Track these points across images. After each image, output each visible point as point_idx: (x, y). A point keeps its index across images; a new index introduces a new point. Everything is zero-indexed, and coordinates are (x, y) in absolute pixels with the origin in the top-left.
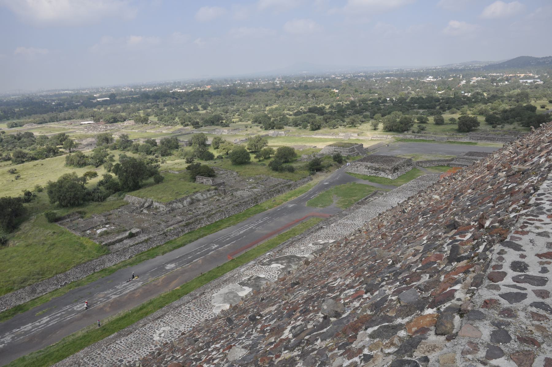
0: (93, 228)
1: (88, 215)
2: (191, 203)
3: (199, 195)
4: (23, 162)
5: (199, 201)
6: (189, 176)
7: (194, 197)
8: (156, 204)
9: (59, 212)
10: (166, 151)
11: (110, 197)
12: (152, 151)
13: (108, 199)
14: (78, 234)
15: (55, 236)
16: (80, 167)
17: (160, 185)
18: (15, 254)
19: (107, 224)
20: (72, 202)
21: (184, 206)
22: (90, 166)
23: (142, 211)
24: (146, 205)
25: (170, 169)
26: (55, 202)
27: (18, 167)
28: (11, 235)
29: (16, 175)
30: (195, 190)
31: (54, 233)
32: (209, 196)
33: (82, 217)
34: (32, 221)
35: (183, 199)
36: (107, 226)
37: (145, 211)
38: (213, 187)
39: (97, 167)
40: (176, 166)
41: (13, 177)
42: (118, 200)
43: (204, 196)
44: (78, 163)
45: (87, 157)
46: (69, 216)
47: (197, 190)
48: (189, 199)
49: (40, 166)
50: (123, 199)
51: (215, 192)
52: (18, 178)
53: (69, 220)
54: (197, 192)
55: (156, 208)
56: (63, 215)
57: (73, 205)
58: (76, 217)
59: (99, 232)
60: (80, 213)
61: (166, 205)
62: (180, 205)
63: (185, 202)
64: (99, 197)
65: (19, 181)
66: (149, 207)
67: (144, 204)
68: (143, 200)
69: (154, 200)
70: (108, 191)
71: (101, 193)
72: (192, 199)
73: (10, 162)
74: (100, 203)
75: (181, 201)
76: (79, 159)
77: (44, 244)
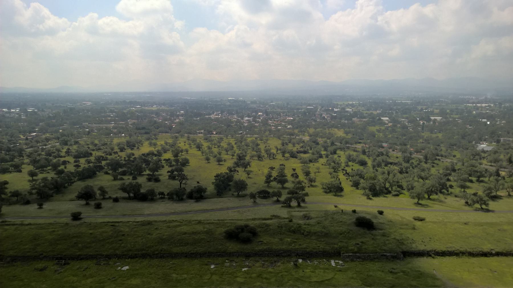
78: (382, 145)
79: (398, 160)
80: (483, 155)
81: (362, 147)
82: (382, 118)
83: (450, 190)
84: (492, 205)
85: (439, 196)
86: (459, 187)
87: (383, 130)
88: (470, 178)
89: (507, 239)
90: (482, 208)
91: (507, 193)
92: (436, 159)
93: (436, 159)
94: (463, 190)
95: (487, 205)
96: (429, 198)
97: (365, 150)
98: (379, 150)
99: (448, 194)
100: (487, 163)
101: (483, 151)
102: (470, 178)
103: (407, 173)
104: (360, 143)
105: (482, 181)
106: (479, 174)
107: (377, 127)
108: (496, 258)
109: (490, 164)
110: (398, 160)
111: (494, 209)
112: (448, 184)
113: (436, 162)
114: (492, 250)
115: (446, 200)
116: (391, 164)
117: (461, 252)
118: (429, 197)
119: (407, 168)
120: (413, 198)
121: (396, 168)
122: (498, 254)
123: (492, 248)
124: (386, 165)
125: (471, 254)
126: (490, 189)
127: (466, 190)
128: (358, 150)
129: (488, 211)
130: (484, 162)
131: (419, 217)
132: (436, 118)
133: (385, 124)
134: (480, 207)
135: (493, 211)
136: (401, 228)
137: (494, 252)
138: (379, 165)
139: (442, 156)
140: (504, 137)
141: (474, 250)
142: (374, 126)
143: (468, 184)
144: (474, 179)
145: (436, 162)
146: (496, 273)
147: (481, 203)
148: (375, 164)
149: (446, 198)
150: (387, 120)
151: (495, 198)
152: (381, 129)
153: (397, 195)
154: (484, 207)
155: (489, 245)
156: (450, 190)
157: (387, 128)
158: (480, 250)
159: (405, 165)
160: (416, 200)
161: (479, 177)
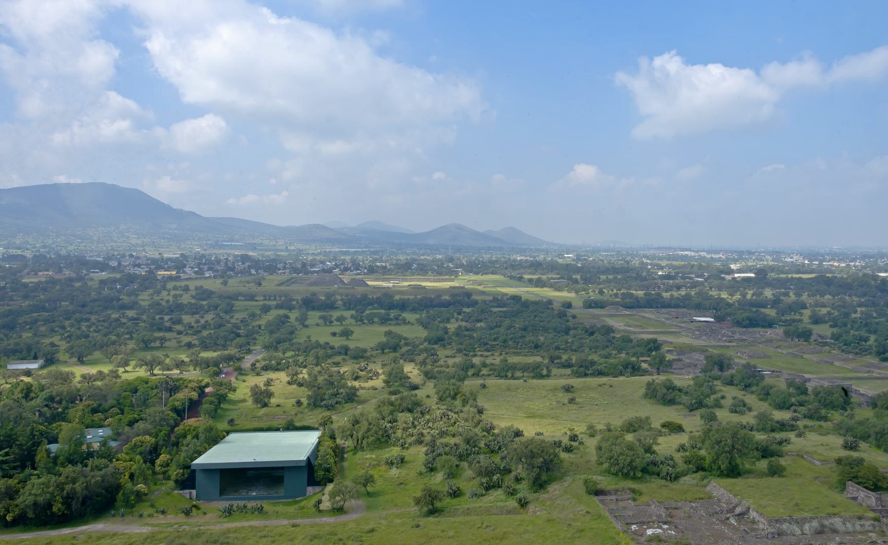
0: (643, 523)
1: (644, 499)
2: (820, 532)
3: (837, 522)
4: (586, 375)
5: (835, 531)
6: (835, 478)
7: (826, 523)
8: (753, 514)
9: (604, 482)
10: (817, 410)
11: (686, 478)
12: (792, 405)
13: (683, 479)
14: (619, 526)
15: (588, 517)
16: (664, 404)
17: (775, 481)
18: (530, 528)
19: (665, 523)
20: (625, 471)
21: (803, 534)
22: (681, 406)
23: (728, 519)
24: (738, 510)
25: (807, 453)
26: (602, 464)
27: (576, 382)
28: (536, 495)
29: (570, 395)
30: (831, 510)
31: (588, 512)
32: (858, 528)
33: (634, 500)
34: (566, 484)
35: (804, 521)
36: (666, 527)
37: (733, 521)
38: (871, 514)
39: (691, 410)
40: (820, 450)
41: (565, 397)
42: (697, 485)
43: (849, 525)
44: (663, 398)
45: (680, 390)
46: (616, 491)
47: (835, 510)
48: (815, 524)
49: (607, 387)
50: (705, 486)
51: (873, 525)
52: (572, 401)
53: (613, 497)
54: (835, 515)
55: (754, 522)
56: (608, 488)
57: (626, 476)
58: (626, 497)
59: (649, 532)
60: (633, 491)
61: (770, 522)
62: (797, 529)
63: (807, 527)
64: (668, 473)
65: (574, 407)
66: (741, 515)
67: (734, 508)
68: (735, 501)
69: (752, 507)
70: (686, 466)
71: (673, 467)
72: (823, 526)
73: (568, 371)
74: (668, 483)
75: (800, 522)
76: (665, 391)
77: (570, 525)
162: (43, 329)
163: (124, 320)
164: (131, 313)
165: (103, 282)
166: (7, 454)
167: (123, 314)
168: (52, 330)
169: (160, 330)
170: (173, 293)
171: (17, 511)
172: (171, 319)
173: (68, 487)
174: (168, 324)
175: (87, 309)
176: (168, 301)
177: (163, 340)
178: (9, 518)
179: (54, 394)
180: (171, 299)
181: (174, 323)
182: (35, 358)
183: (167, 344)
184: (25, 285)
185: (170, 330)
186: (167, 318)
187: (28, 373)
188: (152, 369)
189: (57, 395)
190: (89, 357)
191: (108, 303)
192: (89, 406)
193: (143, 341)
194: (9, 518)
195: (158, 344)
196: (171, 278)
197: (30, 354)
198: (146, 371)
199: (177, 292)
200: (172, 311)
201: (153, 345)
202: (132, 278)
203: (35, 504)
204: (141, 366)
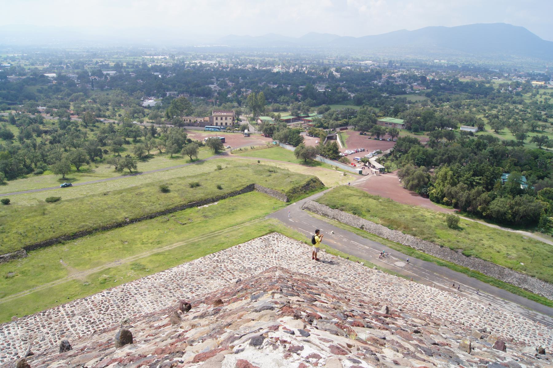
78: (36, 109)
79: (54, 126)
80: (146, 110)
81: (10, 114)
82: (46, 75)
83: (105, 156)
84: (140, 166)
85: (90, 166)
86: (112, 151)
87: (46, 90)
88: (127, 139)
89: (142, 203)
90: (131, 172)
91: (159, 151)
92: (98, 121)
93: (98, 121)
94: (117, 154)
95: (135, 167)
96: (78, 171)
97: (13, 117)
98: (32, 116)
99: (101, 162)
100: (148, 121)
101: (149, 107)
102: (127, 139)
103: (59, 142)
104: (9, 109)
105: (139, 141)
106: (134, 134)
107: (38, 87)
108: (131, 226)
109: (151, 121)
110: (54, 126)
111: (142, 171)
112: (103, 149)
113: (97, 124)
114: (126, 218)
115: (97, 170)
116: (46, 132)
117: (94, 229)
118: (78, 168)
119: (60, 136)
120: (57, 173)
121: (49, 137)
122: (132, 221)
123: (127, 216)
124: (39, 136)
125: (105, 229)
126: (139, 149)
127: (120, 154)
128: (5, 118)
129: (136, 173)
130: (146, 119)
131: (52, 198)
132: (108, 72)
133: (49, 81)
134: (129, 171)
135: (140, 173)
136: (27, 217)
137: (128, 220)
138: (29, 136)
139: (105, 116)
140: (170, 91)
141: (108, 223)
142: (34, 85)
143: (125, 146)
144: (131, 140)
145: (97, 124)
146: (126, 243)
147: (128, 167)
148: (23, 135)
149: (97, 167)
150: (53, 77)
151: (145, 158)
152: (43, 88)
153: (41, 173)
154: (132, 170)
155: (124, 214)
156: (105, 156)
157: (50, 87)
158: (114, 221)
159: (60, 132)
160: (61, 176)
161: (135, 137)
162: (474, 109)
163: (516, 110)
164: (520, 107)
165: (501, 85)
166: (480, 180)
167: (516, 107)
168: (479, 111)
169: (540, 120)
170: (544, 97)
171: (488, 212)
172: (546, 114)
173: (516, 208)
174: (544, 117)
175: (495, 101)
176: (541, 102)
177: (544, 127)
178: (484, 214)
179: (495, 150)
180: (543, 101)
181: (548, 117)
182: (473, 126)
183: (546, 130)
184: (461, 83)
185: (546, 121)
186: (543, 113)
187: (471, 134)
188: (540, 145)
189: (496, 151)
190: (502, 131)
191: (506, 98)
192: (513, 161)
193: (532, 126)
194: (484, 214)
195: (540, 129)
196: (541, 87)
197: (470, 122)
198: (537, 145)
199: (548, 97)
200: (545, 109)
201: (537, 129)
202: (518, 84)
203: (499, 211)
204: (535, 141)
